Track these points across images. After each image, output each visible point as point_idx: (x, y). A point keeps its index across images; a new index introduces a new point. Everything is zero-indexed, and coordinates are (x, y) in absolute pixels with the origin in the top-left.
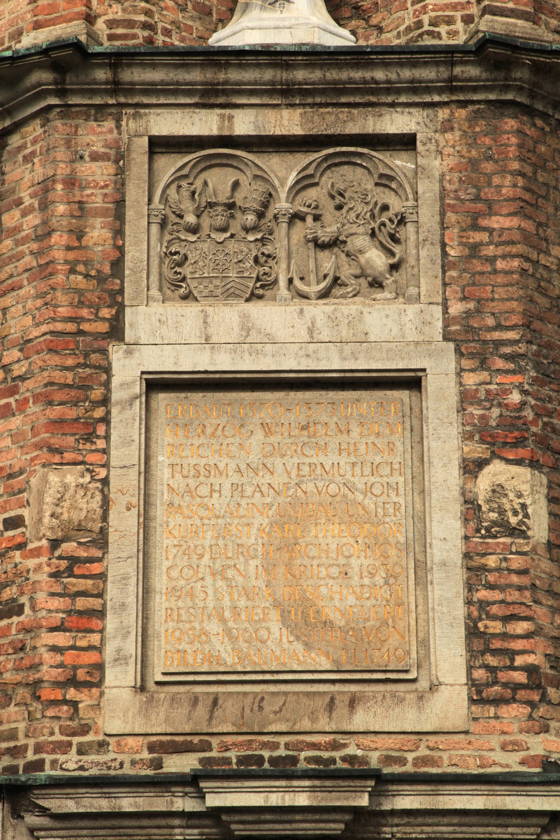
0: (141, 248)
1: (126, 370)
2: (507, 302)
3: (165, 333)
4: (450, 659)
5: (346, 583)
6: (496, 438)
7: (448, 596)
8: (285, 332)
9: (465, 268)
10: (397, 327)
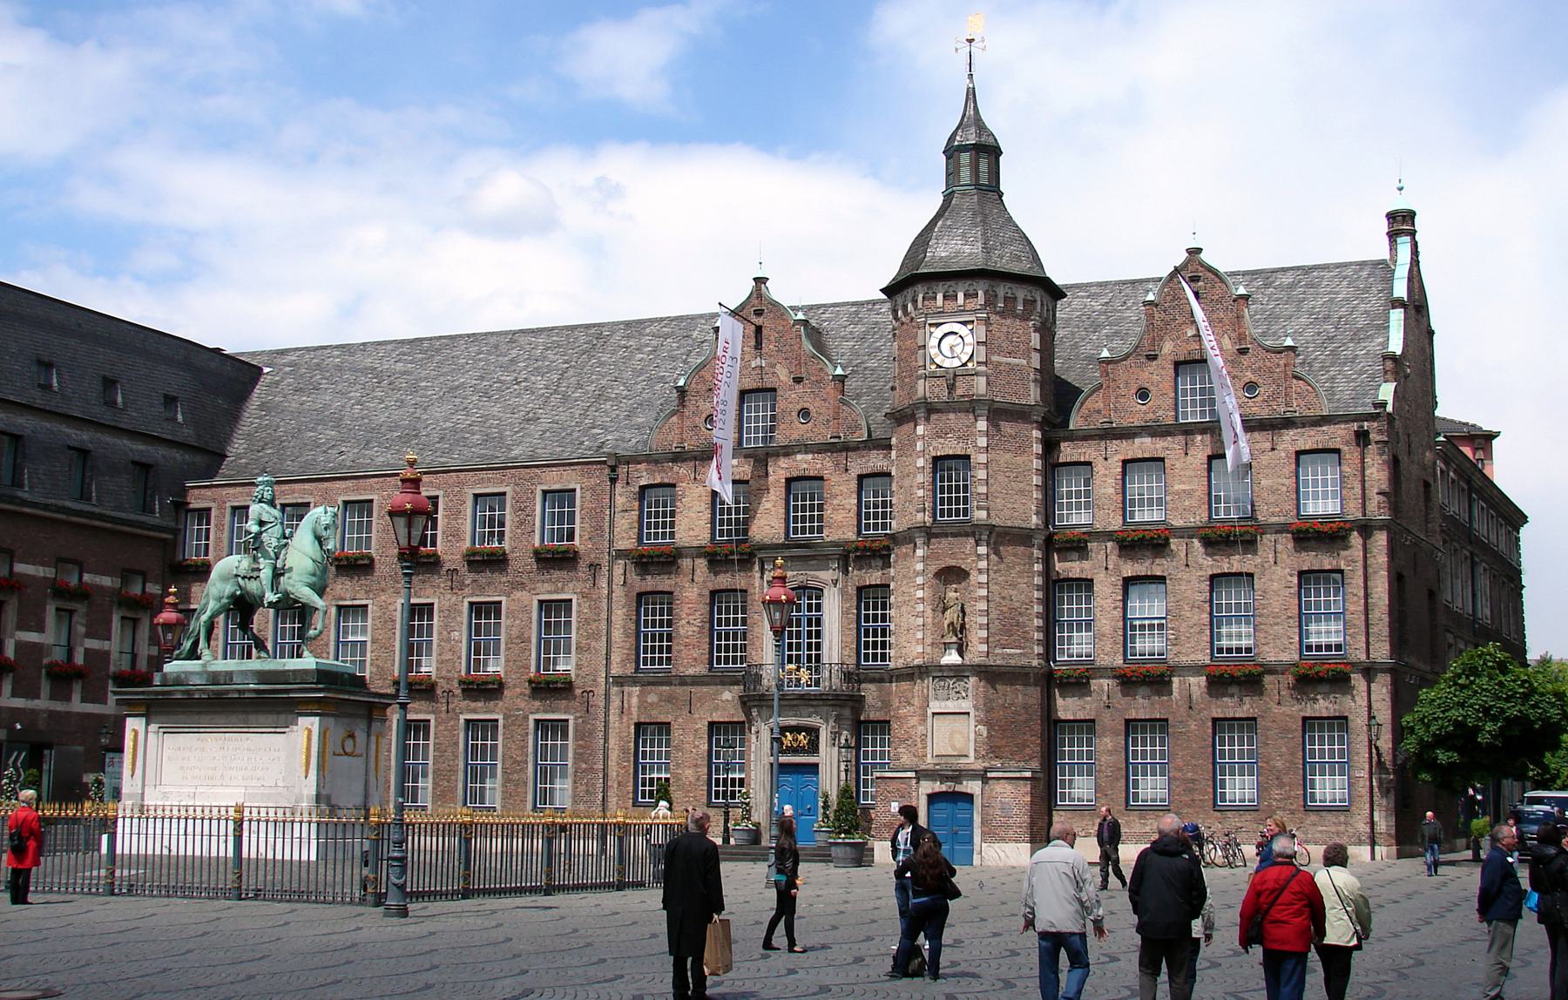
0: (931, 692)
1: (929, 712)
2: (981, 701)
3: (935, 706)
4: (972, 754)
5: (959, 743)
6: (979, 722)
7: (972, 745)
8: (951, 706)
9: (976, 696)
10: (966, 705)
